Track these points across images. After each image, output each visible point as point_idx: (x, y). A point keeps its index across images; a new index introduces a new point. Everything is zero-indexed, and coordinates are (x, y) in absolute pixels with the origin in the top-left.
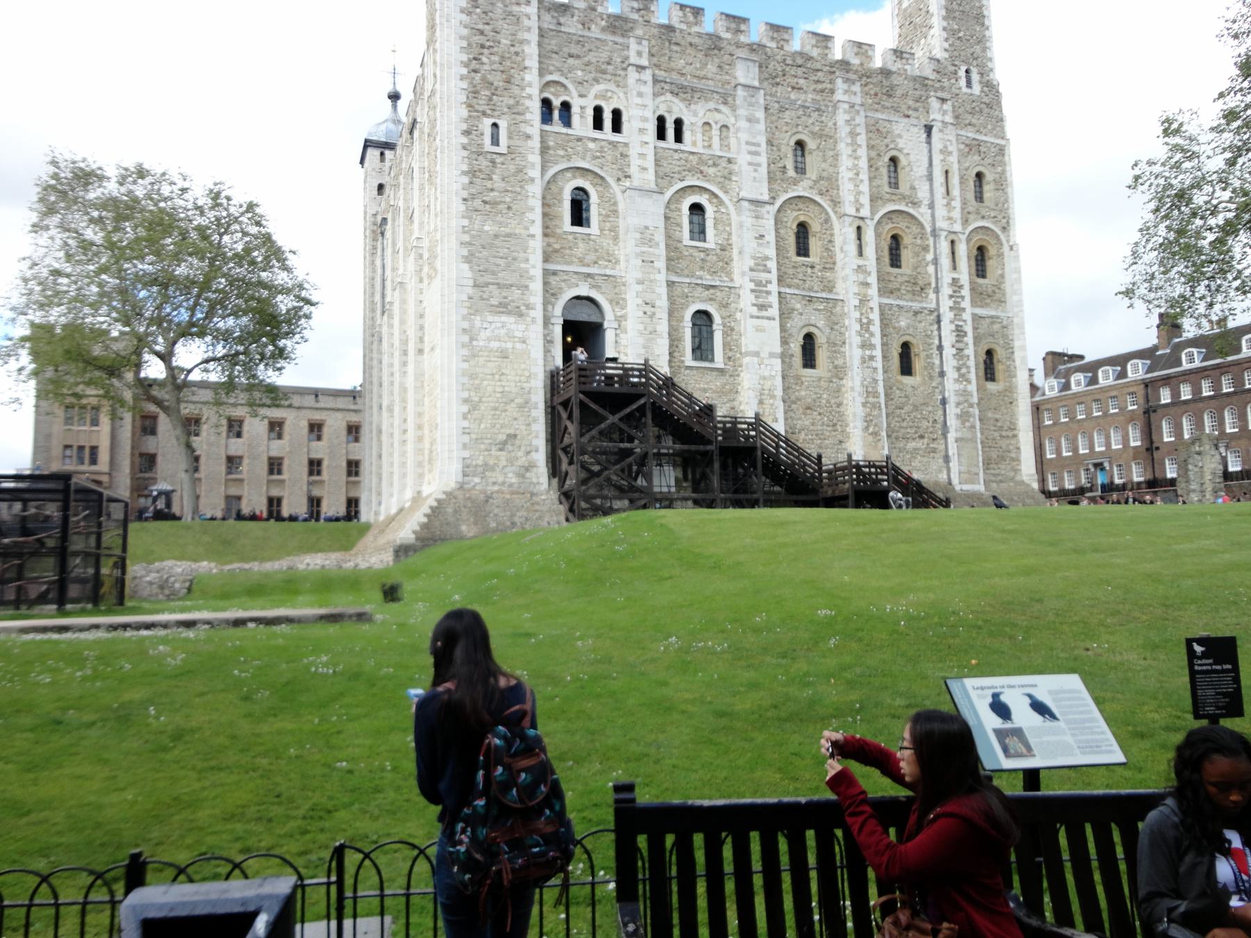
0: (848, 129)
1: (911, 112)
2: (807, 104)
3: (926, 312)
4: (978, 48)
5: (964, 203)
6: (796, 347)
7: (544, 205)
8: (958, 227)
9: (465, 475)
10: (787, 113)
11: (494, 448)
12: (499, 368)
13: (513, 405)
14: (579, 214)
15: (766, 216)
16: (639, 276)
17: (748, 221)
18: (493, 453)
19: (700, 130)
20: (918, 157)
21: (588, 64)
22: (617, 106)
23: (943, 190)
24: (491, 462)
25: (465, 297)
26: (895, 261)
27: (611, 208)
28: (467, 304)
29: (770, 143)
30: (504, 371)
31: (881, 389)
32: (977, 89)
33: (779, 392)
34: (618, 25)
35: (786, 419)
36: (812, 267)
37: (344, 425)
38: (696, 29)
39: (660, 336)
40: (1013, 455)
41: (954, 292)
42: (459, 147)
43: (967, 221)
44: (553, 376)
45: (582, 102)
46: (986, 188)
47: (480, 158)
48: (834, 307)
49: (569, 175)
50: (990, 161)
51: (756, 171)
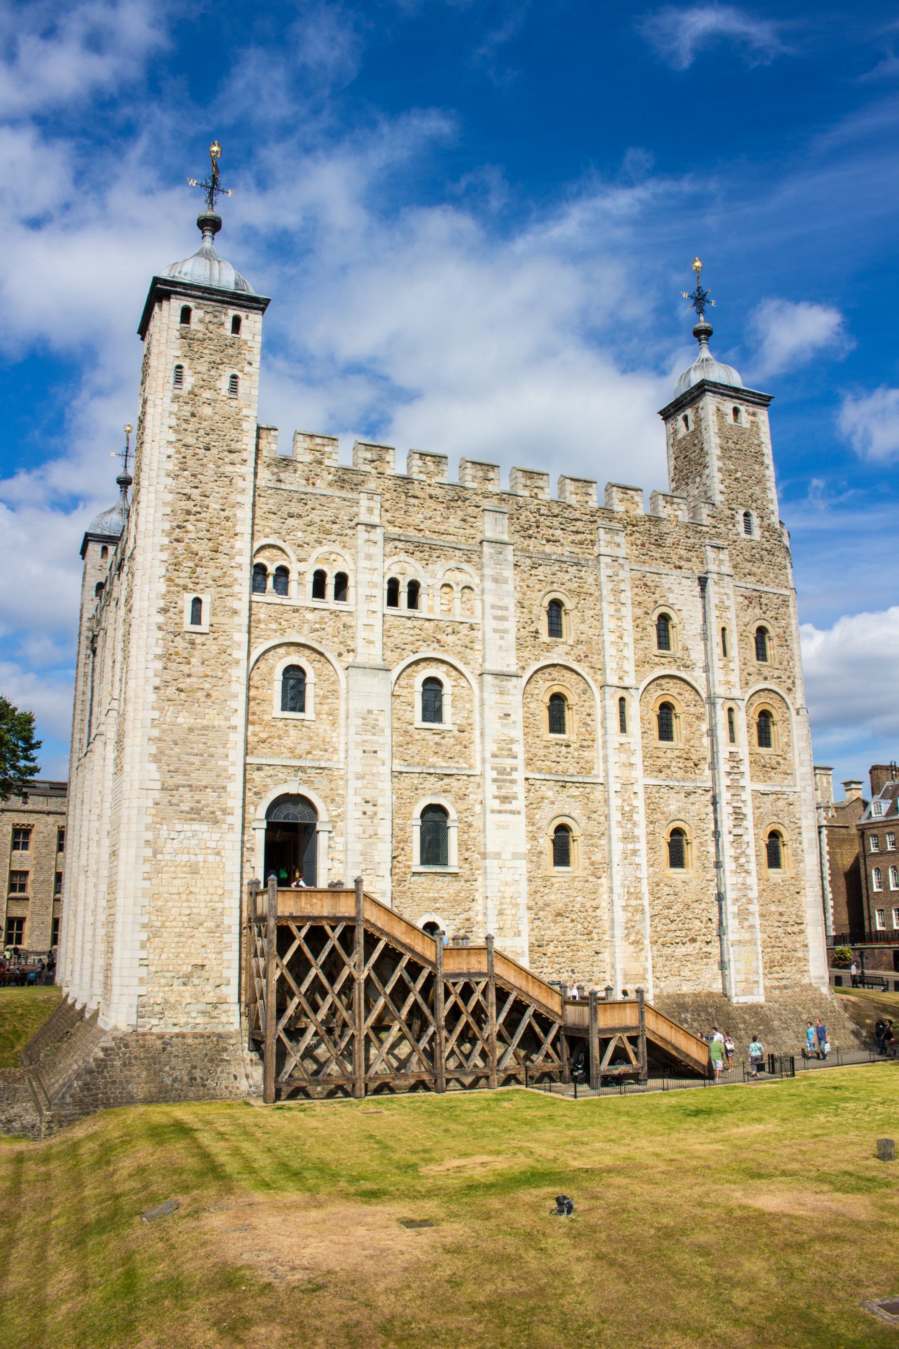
0: (610, 586)
1: (682, 563)
2: (564, 559)
3: (700, 791)
4: (757, 490)
9: (140, 1016)
11: (176, 982)
13: (201, 929)
15: (513, 691)
16: (359, 769)
17: (491, 697)
18: (175, 988)
19: (438, 593)
20: (691, 613)
24: (172, 1000)
25: (150, 804)
26: (666, 733)
27: (331, 687)
28: (153, 811)
30: (192, 889)
31: (645, 888)
32: (757, 534)
33: (523, 901)
35: (532, 930)
38: (439, 479)
40: (800, 954)
42: (154, 627)
43: (747, 684)
45: (302, 567)
46: (768, 644)
47: (178, 638)
49: (282, 651)
50: (773, 614)
51: (502, 638)
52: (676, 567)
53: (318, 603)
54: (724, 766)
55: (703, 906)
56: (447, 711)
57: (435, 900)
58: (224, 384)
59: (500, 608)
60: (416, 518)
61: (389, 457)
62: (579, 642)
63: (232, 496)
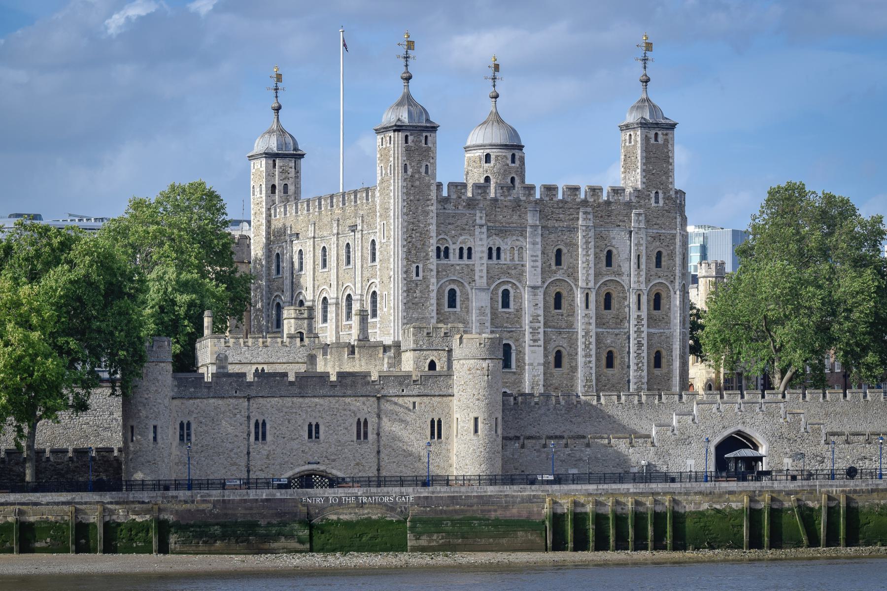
5: (648, 270)
6: (551, 358)
7: (438, 299)
8: (643, 287)
14: (452, 303)
15: (539, 294)
21: (458, 226)
23: (636, 266)
26: (608, 306)
29: (543, 253)
33: (541, 383)
34: (471, 204)
36: (562, 315)
38: (509, 198)
41: (638, 322)
46: (663, 259)
48: (573, 335)
49: (447, 283)
50: (666, 244)
53: (461, 262)
54: (633, 322)
56: (512, 303)
57: (506, 383)
58: (423, 170)
59: (535, 256)
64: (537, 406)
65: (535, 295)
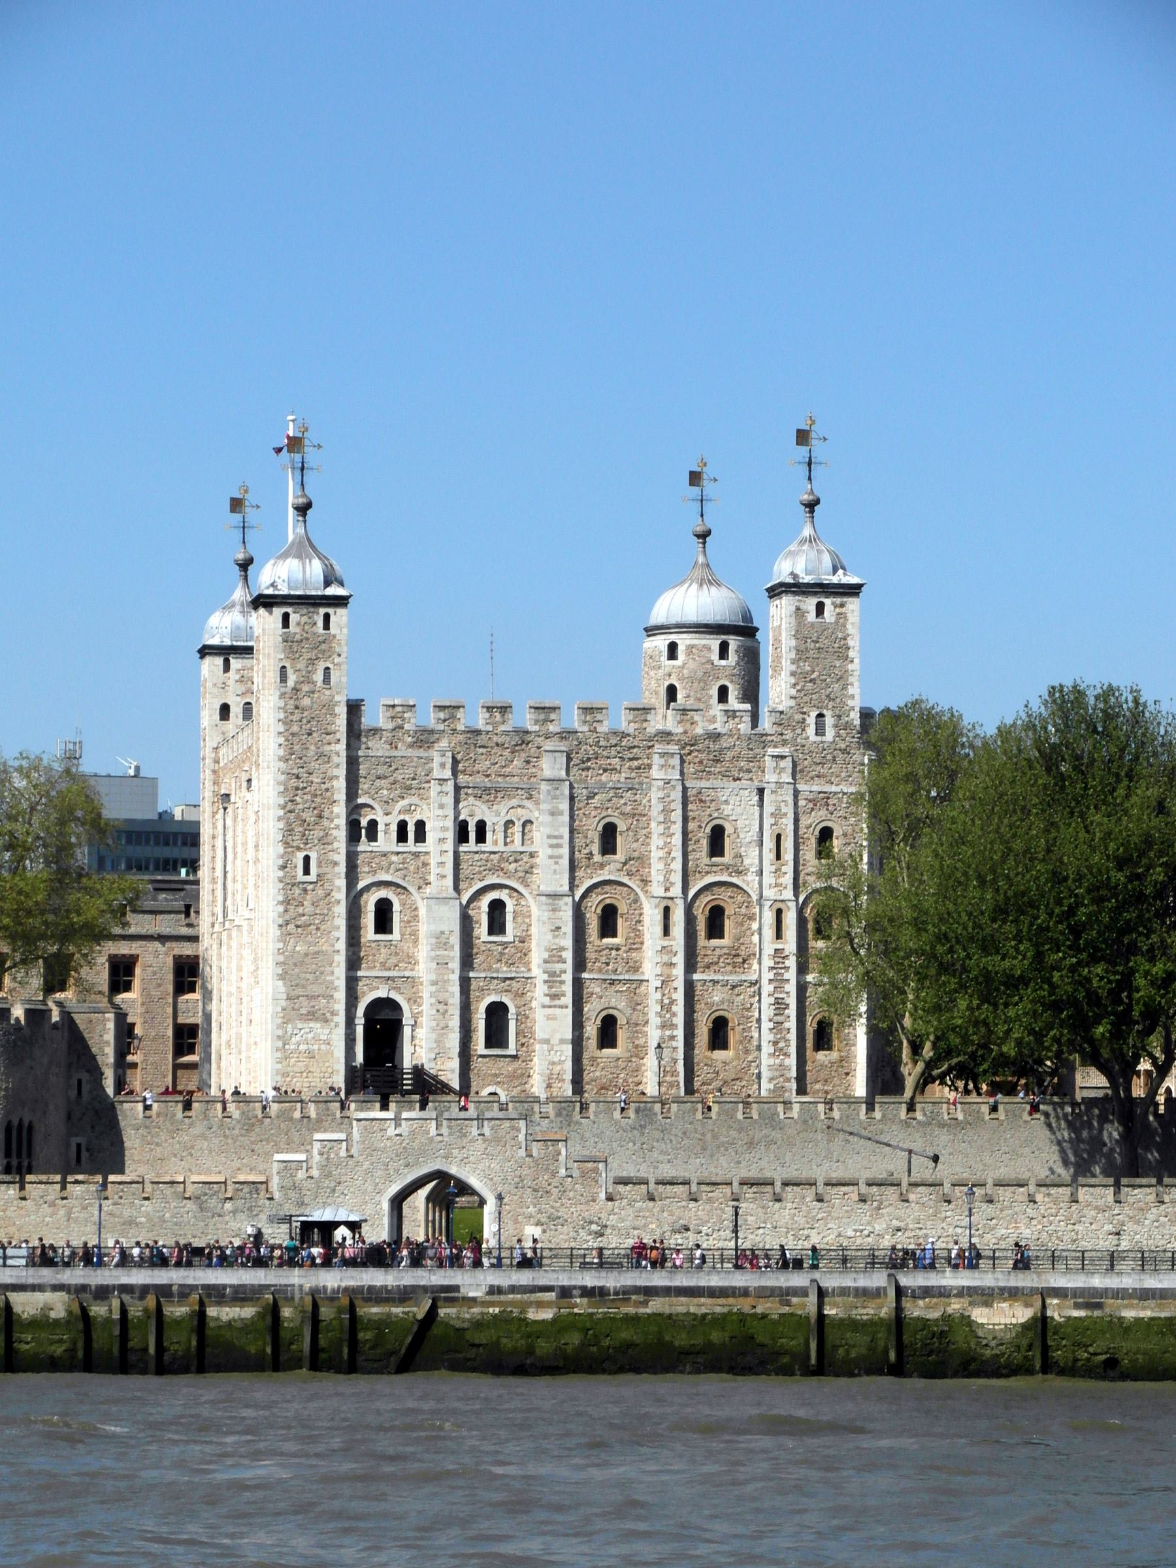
8: (789, 894)
10: (597, 797)
12: (307, 1066)
14: (383, 922)
15: (564, 908)
16: (433, 977)
20: (747, 822)
22: (418, 817)
23: (773, 856)
33: (568, 1076)
34: (425, 738)
36: (618, 949)
37: (170, 961)
39: (452, 1030)
44: (351, 1071)
45: (387, 819)
51: (556, 863)
52: (735, 780)
53: (402, 848)
55: (744, 1083)
57: (496, 1075)
58: (319, 677)
59: (556, 837)
60: (483, 765)
61: (460, 714)
62: (630, 859)
63: (330, 771)
64: (187, 1120)
65: (554, 910)
